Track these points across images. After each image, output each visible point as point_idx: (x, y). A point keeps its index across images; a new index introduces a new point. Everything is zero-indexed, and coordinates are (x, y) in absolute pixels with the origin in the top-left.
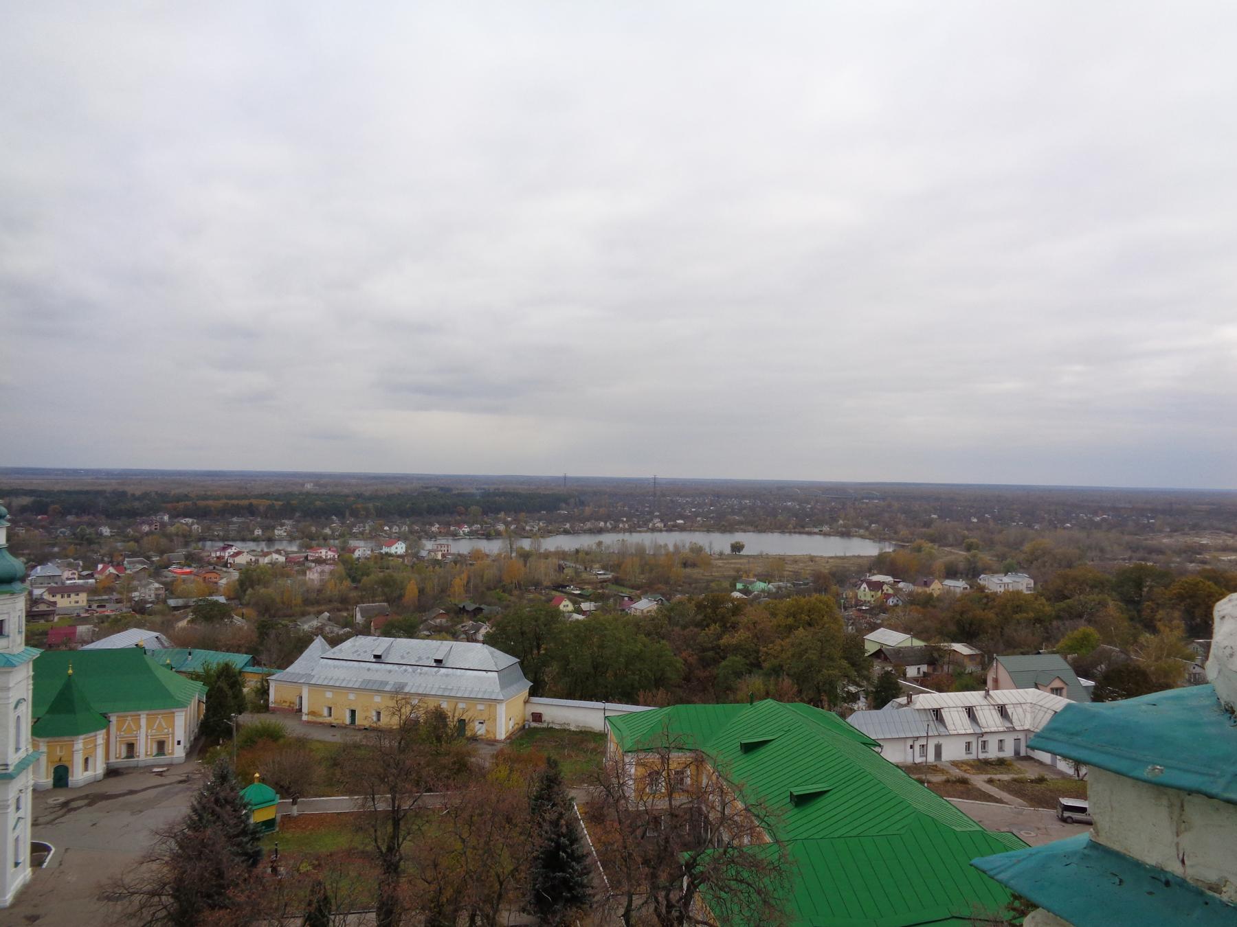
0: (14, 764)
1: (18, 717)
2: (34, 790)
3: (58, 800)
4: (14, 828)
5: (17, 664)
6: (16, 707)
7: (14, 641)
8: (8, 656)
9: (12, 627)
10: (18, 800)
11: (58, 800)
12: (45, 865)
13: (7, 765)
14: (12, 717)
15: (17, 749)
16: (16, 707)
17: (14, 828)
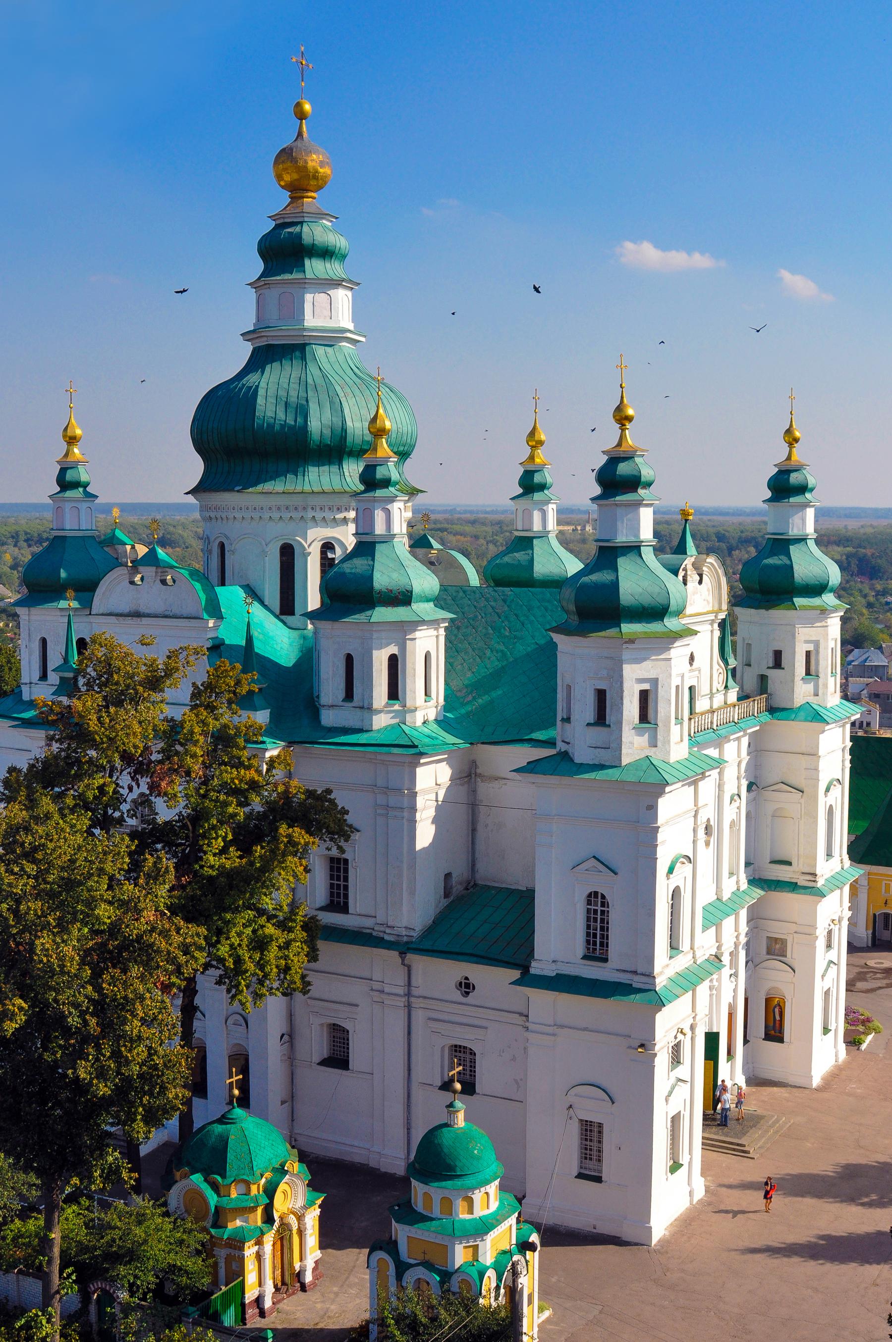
0: (826, 877)
1: (831, 806)
2: (850, 944)
3: (883, 963)
4: (823, 976)
5: (828, 720)
6: (828, 790)
7: (826, 686)
8: (815, 707)
9: (822, 663)
10: (830, 933)
11: (883, 963)
12: (864, 1047)
13: (815, 875)
14: (823, 803)
15: (829, 855)
16: (828, 790)
17: (823, 976)
